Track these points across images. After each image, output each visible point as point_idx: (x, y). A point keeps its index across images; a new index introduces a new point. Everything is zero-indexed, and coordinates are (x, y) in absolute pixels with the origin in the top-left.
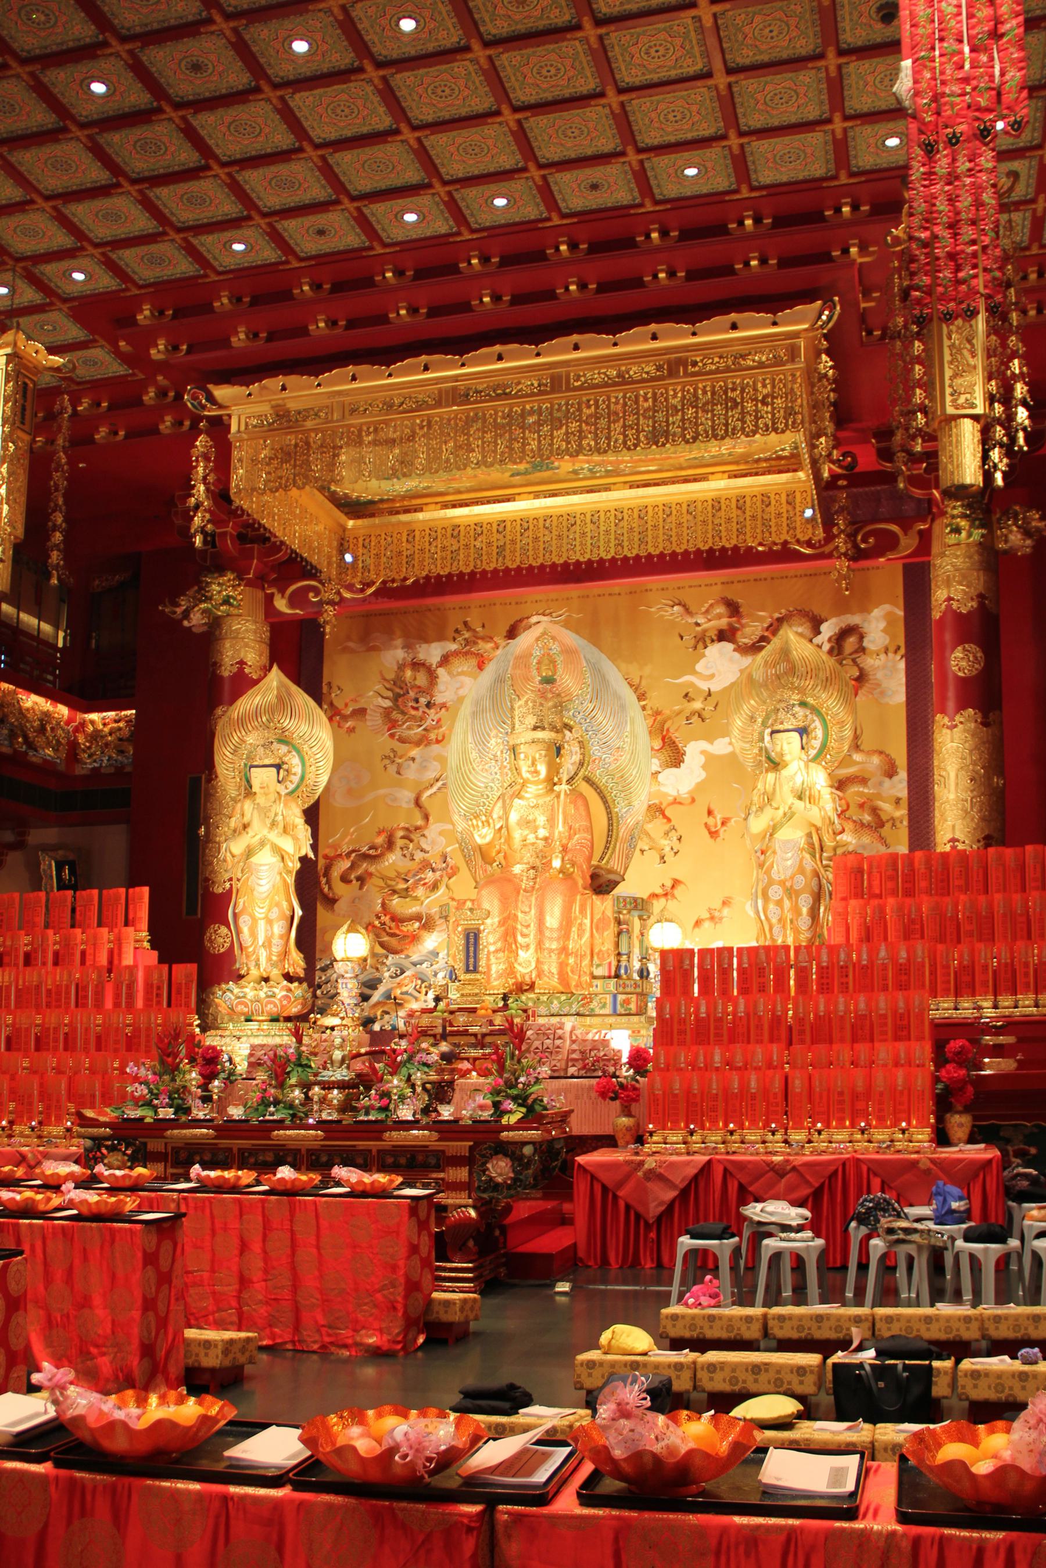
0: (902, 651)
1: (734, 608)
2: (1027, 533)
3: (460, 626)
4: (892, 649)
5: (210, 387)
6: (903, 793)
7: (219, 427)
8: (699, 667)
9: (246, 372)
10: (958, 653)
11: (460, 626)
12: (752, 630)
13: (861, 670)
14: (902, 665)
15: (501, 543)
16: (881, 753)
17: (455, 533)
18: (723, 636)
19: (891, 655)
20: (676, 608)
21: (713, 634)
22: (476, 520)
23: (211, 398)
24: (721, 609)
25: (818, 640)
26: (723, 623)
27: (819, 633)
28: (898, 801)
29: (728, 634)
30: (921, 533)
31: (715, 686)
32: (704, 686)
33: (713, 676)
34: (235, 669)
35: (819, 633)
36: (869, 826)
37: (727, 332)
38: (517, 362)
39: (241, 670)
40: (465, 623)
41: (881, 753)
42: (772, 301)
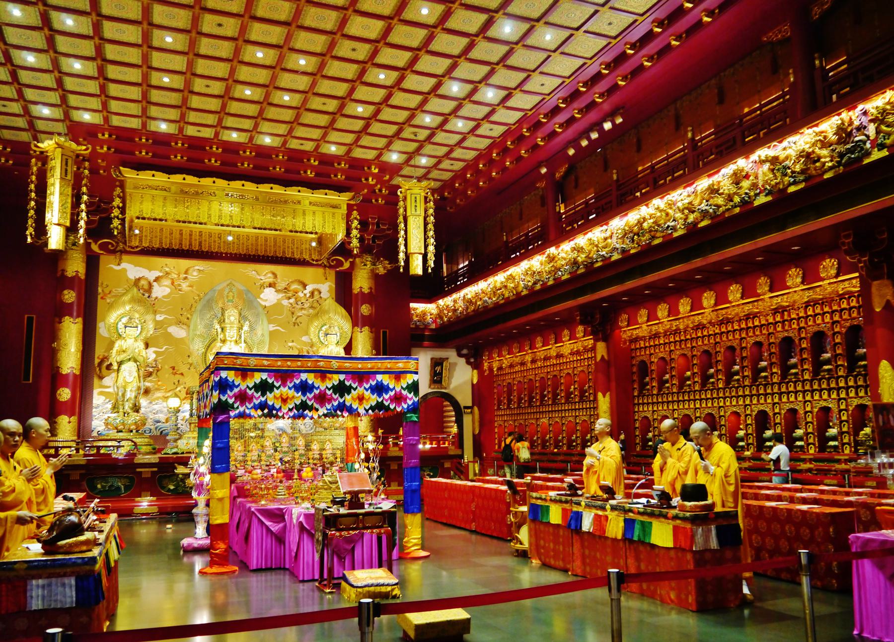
2: (385, 268)
5: (121, 168)
7: (122, 185)
8: (261, 296)
9: (140, 166)
10: (364, 307)
12: (281, 285)
18: (270, 285)
21: (268, 284)
23: (120, 172)
24: (270, 275)
25: (305, 292)
26: (271, 280)
31: (267, 304)
32: (263, 303)
33: (266, 300)
39: (77, 275)
42: (340, 188)
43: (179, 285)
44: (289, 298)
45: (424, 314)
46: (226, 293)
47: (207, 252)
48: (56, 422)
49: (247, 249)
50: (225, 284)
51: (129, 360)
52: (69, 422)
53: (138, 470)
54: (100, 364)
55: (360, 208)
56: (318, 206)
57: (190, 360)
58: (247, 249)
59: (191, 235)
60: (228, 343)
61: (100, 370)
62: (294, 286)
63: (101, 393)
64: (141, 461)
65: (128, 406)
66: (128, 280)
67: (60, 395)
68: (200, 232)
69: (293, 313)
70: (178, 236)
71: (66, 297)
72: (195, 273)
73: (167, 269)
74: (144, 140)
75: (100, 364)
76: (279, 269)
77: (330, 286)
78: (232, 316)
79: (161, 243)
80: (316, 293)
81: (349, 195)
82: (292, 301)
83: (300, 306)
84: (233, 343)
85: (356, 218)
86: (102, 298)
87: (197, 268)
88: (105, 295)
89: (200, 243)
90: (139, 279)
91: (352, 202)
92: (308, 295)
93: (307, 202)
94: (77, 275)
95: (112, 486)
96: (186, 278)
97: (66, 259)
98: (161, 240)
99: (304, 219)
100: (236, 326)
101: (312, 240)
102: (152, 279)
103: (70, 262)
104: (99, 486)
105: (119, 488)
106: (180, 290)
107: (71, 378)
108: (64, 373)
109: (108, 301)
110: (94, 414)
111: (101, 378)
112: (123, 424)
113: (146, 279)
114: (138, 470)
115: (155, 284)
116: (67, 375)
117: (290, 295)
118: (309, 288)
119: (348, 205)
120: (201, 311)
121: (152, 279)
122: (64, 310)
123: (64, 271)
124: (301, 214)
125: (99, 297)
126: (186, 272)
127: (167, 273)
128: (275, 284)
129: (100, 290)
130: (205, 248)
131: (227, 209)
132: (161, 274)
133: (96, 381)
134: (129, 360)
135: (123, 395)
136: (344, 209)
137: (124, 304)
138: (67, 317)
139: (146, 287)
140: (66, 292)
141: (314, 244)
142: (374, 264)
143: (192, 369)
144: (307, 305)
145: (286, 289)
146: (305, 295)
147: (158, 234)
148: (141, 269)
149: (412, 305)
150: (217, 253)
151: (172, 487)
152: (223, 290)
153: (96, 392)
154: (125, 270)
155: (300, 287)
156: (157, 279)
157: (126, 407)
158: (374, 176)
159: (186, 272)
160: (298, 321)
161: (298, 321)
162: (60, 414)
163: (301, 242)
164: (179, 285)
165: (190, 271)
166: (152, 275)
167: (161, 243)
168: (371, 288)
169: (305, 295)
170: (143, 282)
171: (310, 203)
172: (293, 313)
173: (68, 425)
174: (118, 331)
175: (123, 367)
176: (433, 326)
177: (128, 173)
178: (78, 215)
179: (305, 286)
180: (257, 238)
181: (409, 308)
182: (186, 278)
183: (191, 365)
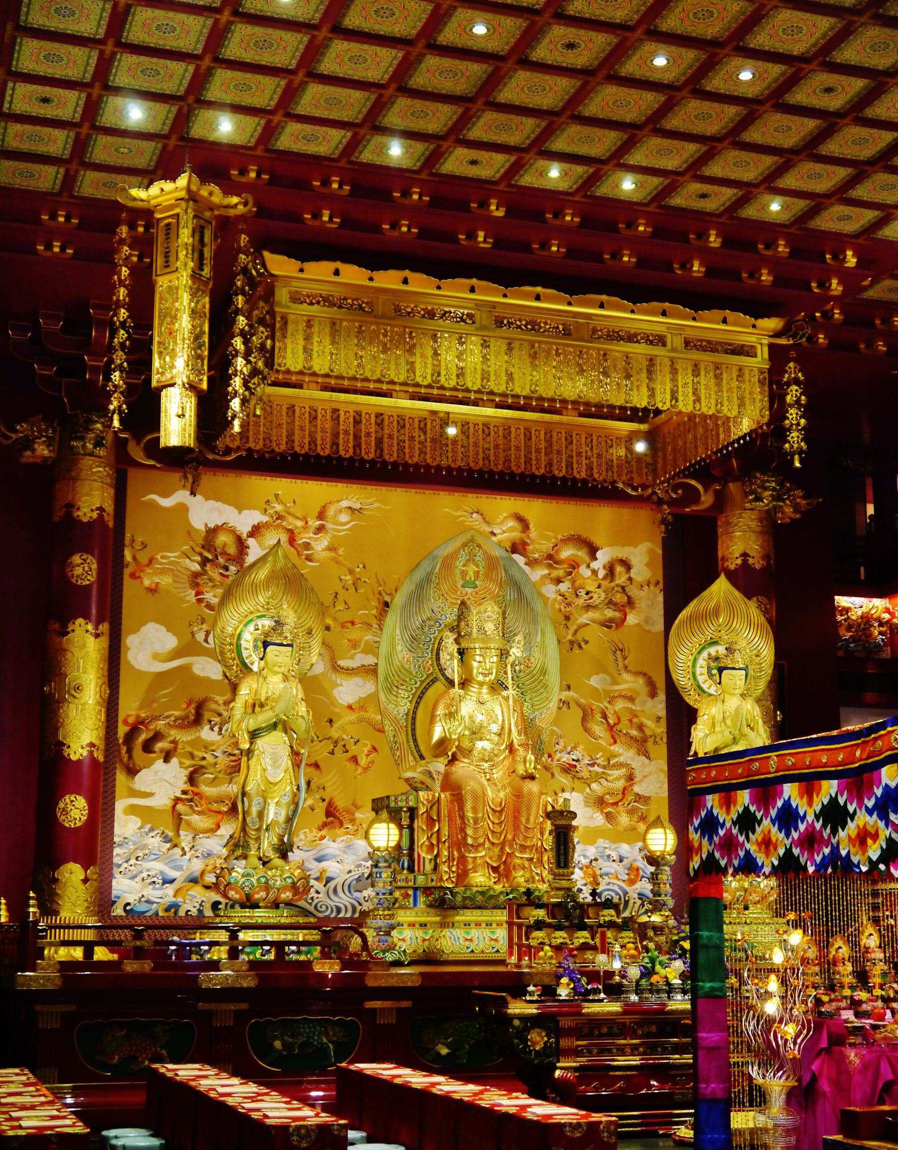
0: (661, 586)
1: (524, 524)
2: (796, 507)
3: (272, 498)
4: (653, 583)
5: (266, 254)
6: (663, 713)
9: (307, 250)
11: (272, 498)
13: (629, 597)
14: (661, 598)
15: (379, 435)
16: (645, 675)
17: (379, 421)
19: (652, 587)
20: (475, 515)
22: (400, 412)
24: (512, 523)
25: (595, 565)
26: (516, 535)
27: (596, 559)
28: (659, 718)
29: (520, 547)
30: (715, 491)
34: (95, 515)
35: (596, 559)
36: (636, 740)
37: (718, 323)
38: (554, 305)
40: (277, 496)
41: (645, 675)
42: (756, 308)
43: (307, 546)
44: (559, 581)
45: (867, 619)
46: (459, 563)
47: (395, 464)
48: (56, 881)
49: (486, 458)
50: (458, 543)
51: (274, 726)
52: (85, 881)
53: (370, 1005)
54: (130, 737)
55: (806, 357)
56: (704, 349)
57: (335, 735)
58: (486, 458)
59: (357, 422)
60: (474, 688)
61: (129, 751)
62: (566, 553)
63: (133, 810)
64: (383, 983)
65: (268, 843)
66: (190, 532)
67: (65, 811)
68: (379, 415)
69: (567, 618)
70: (328, 426)
71: (78, 571)
72: (344, 518)
73: (279, 508)
74: (335, 186)
75: (130, 737)
76: (535, 508)
77: (651, 552)
78: (486, 618)
79: (290, 441)
80: (619, 569)
81: (772, 324)
82: (564, 587)
83: (580, 602)
84: (485, 690)
85: (796, 382)
86: (133, 576)
87: (345, 504)
88: (140, 568)
89: (379, 441)
90: (212, 532)
91: (783, 341)
92: (601, 573)
93: (679, 342)
94: (101, 516)
95: (307, 1044)
96: (320, 529)
97: (76, 479)
98: (290, 434)
99: (674, 380)
100: (496, 644)
101: (631, 438)
102: (244, 529)
103: (84, 487)
104: (278, 1044)
105: (324, 1050)
106: (309, 558)
107: (86, 769)
108: (74, 758)
109: (147, 582)
110: (116, 860)
111: (132, 771)
112: (267, 888)
113: (232, 531)
114: (370, 1005)
115: (251, 542)
116: (79, 761)
117: (561, 573)
118: (603, 556)
119: (771, 347)
120: (404, 608)
121: (244, 529)
122: (67, 605)
123: (71, 506)
124: (667, 369)
125: (127, 572)
126: (321, 516)
127: (280, 517)
128: (524, 544)
129: (128, 555)
130: (391, 455)
131: (468, 359)
132: (265, 519)
133: (121, 777)
134: (274, 726)
135: (261, 815)
136: (761, 360)
137: (254, 589)
138: (80, 621)
139: (232, 550)
140: (77, 559)
141: (640, 447)
142: (777, 498)
143: (339, 750)
144: (599, 597)
145: (550, 557)
146: (595, 572)
147: (284, 420)
148: (219, 504)
149: (842, 601)
150: (417, 466)
151: (444, 1051)
152: (454, 556)
153: (120, 805)
154: (182, 508)
155: (583, 554)
156: (255, 531)
157: (265, 844)
158: (845, 276)
159: (321, 516)
160: (579, 636)
161: (579, 636)
162: (67, 862)
163: (610, 440)
164: (307, 546)
165: (331, 512)
166: (244, 521)
167: (290, 441)
168: (766, 557)
169: (595, 572)
170: (223, 539)
171: (687, 343)
172: (567, 618)
173: (81, 887)
174: (240, 655)
175: (260, 743)
176: (887, 653)
177: (279, 265)
178: (229, 363)
179: (593, 551)
180: (507, 430)
181: (833, 609)
182: (320, 529)
183: (336, 743)
